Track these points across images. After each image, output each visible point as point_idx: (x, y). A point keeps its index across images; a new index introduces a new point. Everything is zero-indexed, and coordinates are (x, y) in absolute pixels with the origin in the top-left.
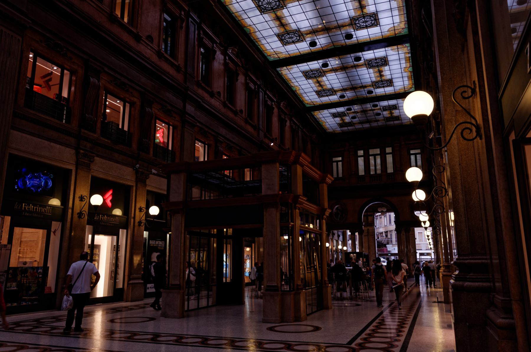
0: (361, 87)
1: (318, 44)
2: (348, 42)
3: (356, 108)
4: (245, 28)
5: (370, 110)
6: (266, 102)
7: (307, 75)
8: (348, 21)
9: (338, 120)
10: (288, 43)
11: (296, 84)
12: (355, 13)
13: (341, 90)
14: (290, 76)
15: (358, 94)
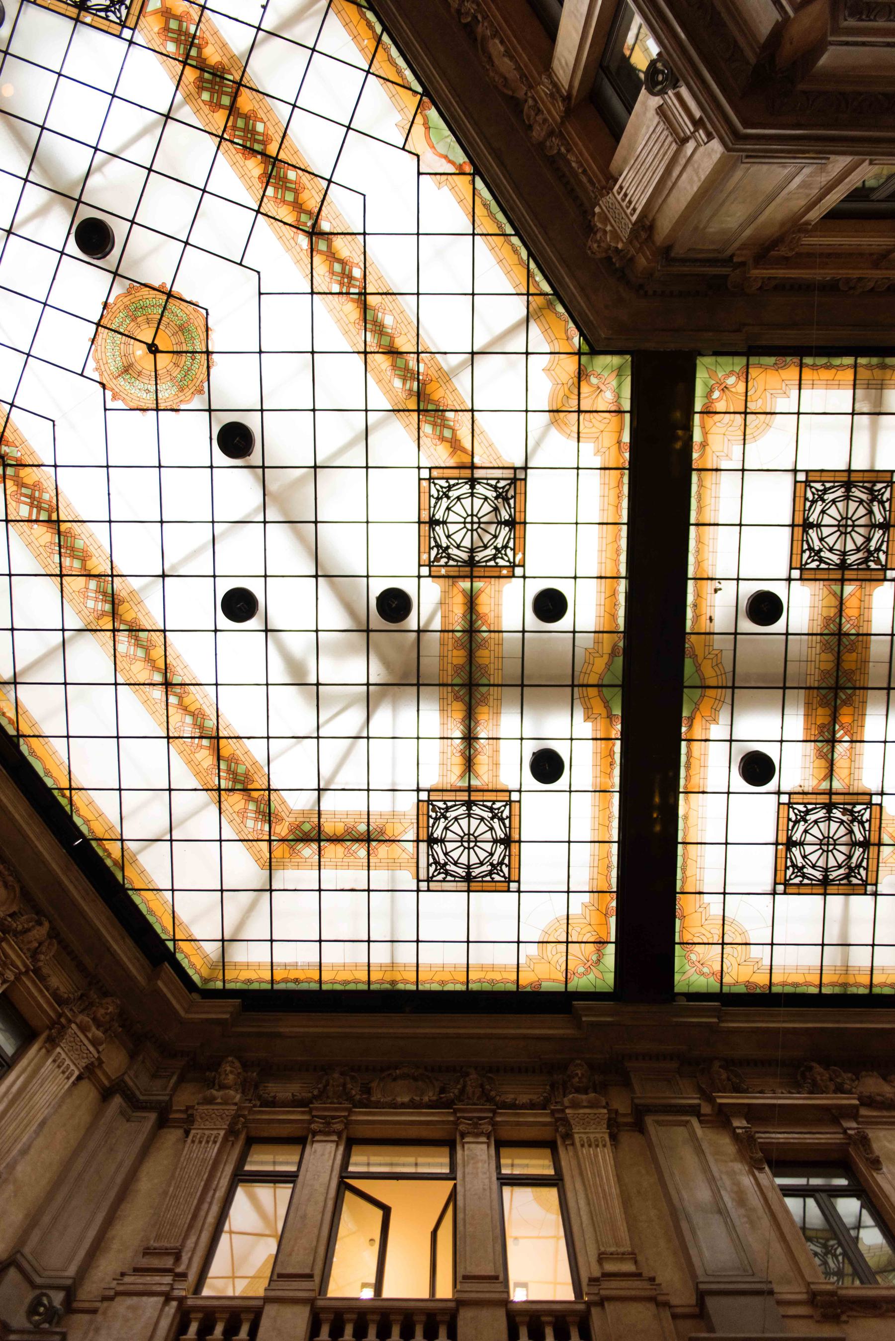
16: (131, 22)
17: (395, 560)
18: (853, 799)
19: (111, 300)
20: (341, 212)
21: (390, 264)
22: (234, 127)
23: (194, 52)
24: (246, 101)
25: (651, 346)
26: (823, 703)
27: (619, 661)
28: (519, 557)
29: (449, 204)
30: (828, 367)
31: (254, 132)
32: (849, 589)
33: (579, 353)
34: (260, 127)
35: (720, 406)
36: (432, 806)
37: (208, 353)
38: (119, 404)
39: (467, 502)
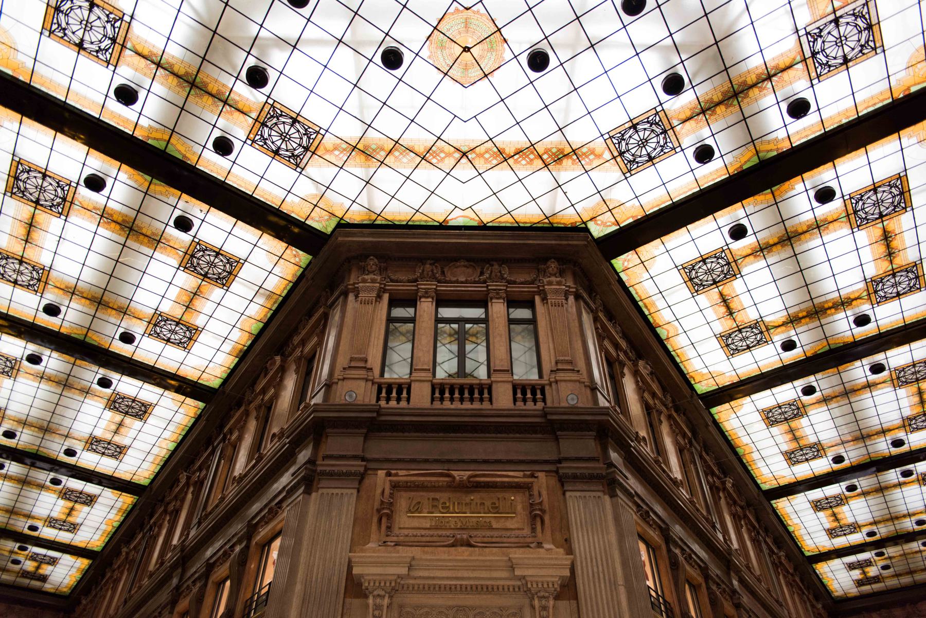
0: (904, 516)
1: (846, 458)
2: (895, 451)
3: (891, 551)
4: (738, 450)
5: (916, 552)
6: (770, 557)
7: (817, 506)
8: (898, 422)
9: (857, 574)
10: (798, 462)
11: (797, 521)
12: (911, 410)
13: (871, 524)
14: (789, 510)
15: (898, 527)
16: (609, 141)
17: (285, 92)
18: (66, 209)
19: (505, 45)
20: (464, 171)
21: (428, 175)
22: (532, 153)
23: (575, 157)
24: (539, 163)
25: (326, 248)
26: (124, 221)
27: (180, 157)
28: (257, 146)
29: (437, 211)
30: (285, 288)
31: (524, 159)
32: (181, 253)
33: (341, 219)
34: (524, 162)
35: (288, 251)
36: (119, 21)
37: (446, 74)
38: (451, 10)
39: (298, 141)
